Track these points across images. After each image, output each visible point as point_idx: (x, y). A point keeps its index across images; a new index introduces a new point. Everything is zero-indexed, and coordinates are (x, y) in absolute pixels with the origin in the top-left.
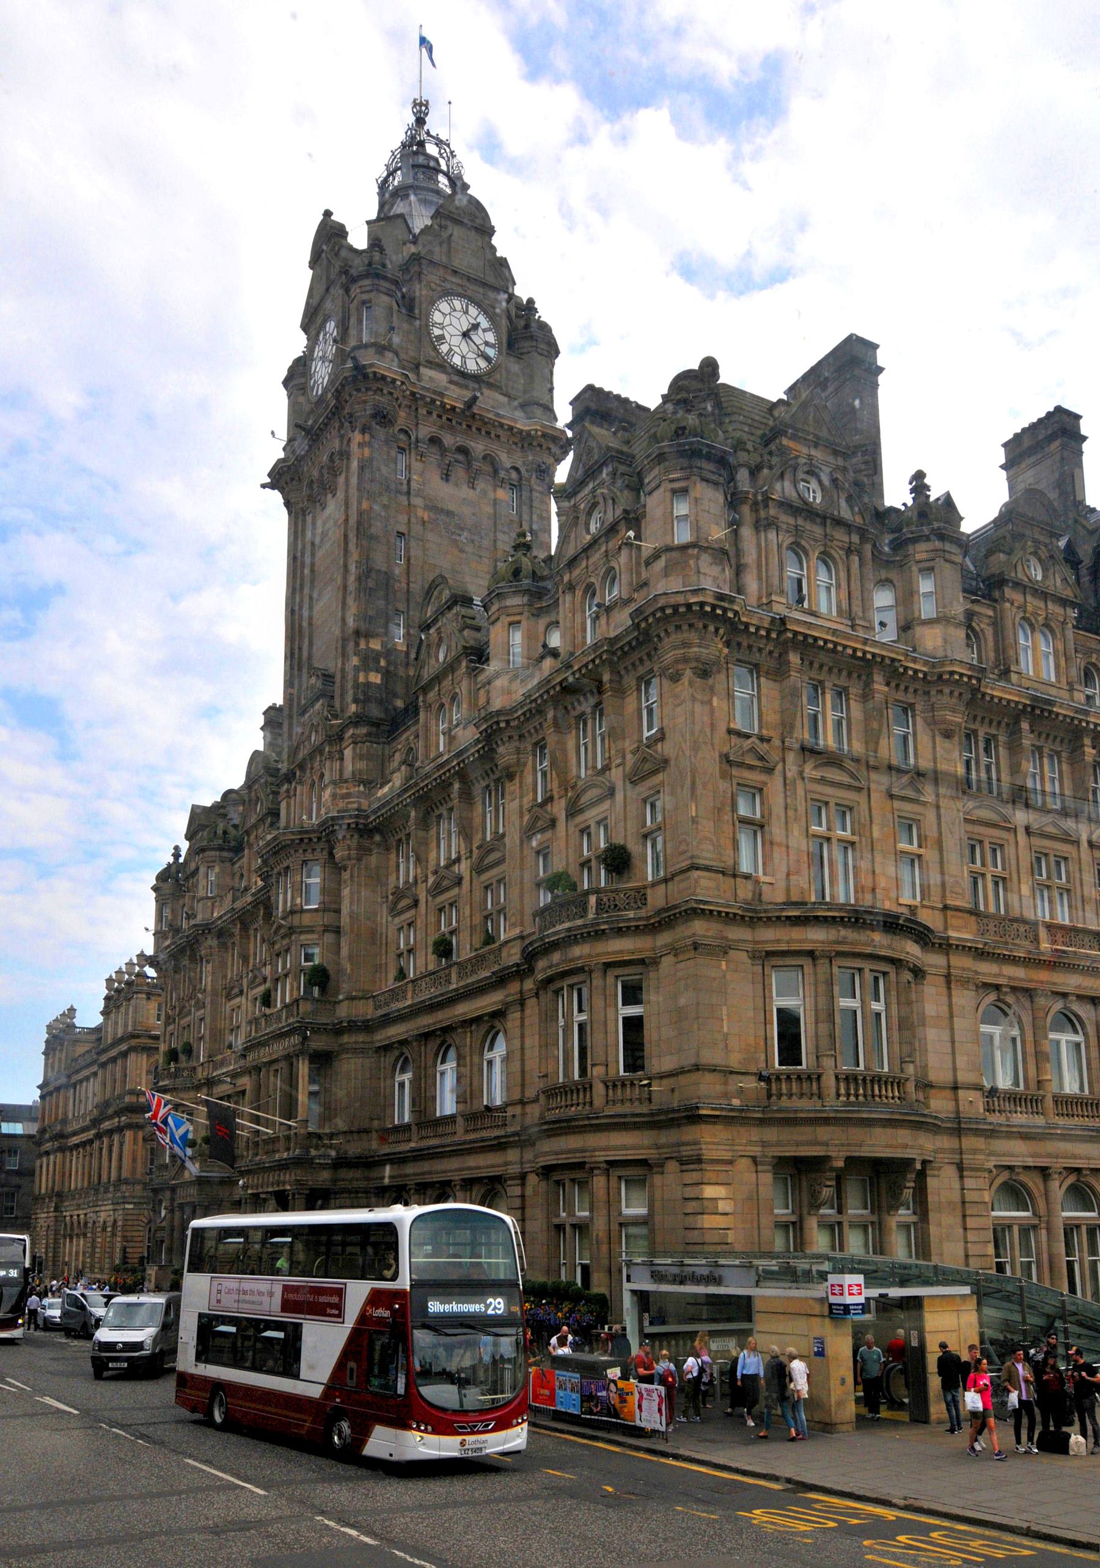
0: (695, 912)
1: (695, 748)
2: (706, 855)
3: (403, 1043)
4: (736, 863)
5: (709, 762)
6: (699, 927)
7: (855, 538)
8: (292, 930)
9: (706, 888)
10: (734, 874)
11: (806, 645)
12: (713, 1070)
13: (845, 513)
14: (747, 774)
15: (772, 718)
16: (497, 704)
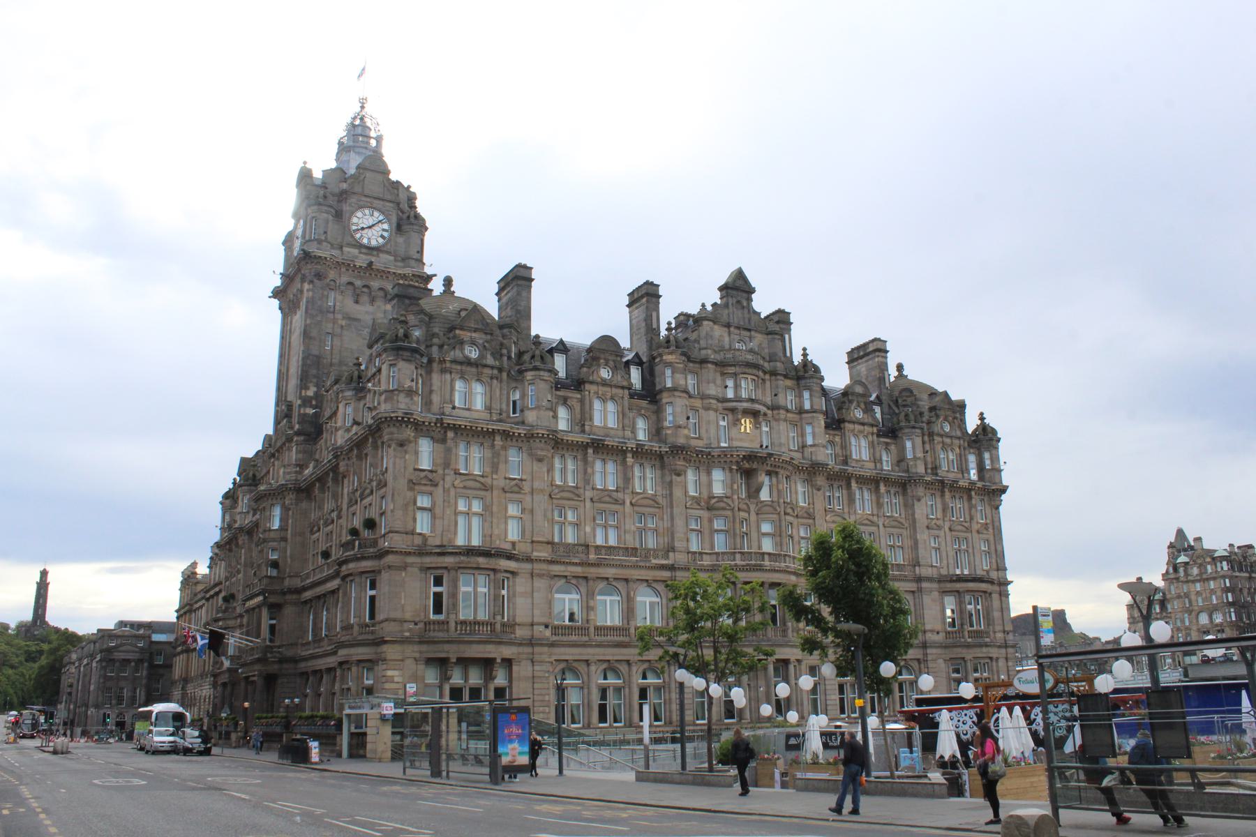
0: (388, 552)
1: (395, 478)
2: (398, 525)
3: (311, 600)
4: (415, 528)
5: (402, 483)
6: (390, 559)
7: (495, 372)
8: (265, 541)
9: (398, 542)
10: (413, 533)
11: (456, 428)
12: (394, 620)
14: (424, 488)
15: (439, 461)
16: (340, 442)
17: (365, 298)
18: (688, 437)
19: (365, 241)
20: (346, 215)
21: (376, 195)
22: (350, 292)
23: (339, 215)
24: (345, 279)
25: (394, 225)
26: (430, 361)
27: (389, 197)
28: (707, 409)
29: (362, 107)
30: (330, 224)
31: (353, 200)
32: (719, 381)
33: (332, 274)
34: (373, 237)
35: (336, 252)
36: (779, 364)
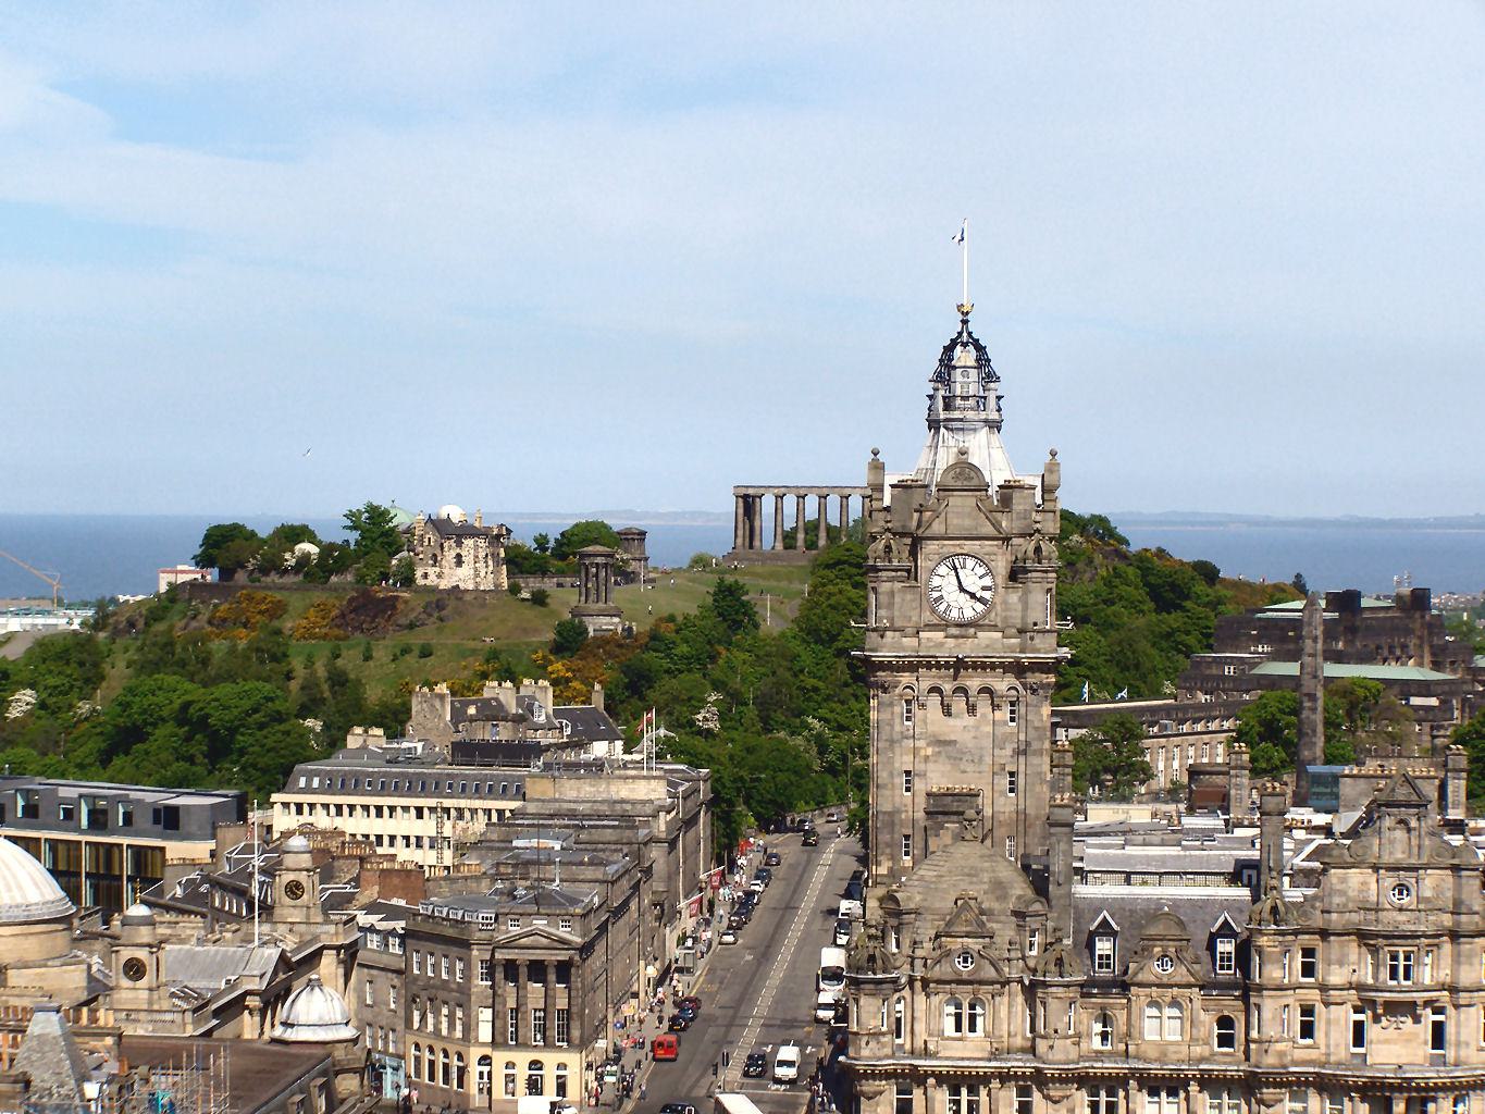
13: (990, 973)
17: (959, 704)
18: (1282, 1054)
19: (954, 614)
20: (923, 576)
21: (966, 535)
22: (935, 699)
23: (912, 574)
24: (925, 685)
25: (1000, 581)
26: (911, 980)
27: (989, 530)
28: (1327, 1004)
29: (965, 322)
30: (897, 599)
31: (931, 547)
32: (1353, 957)
33: (906, 678)
34: (961, 608)
35: (913, 642)
36: (1464, 918)
